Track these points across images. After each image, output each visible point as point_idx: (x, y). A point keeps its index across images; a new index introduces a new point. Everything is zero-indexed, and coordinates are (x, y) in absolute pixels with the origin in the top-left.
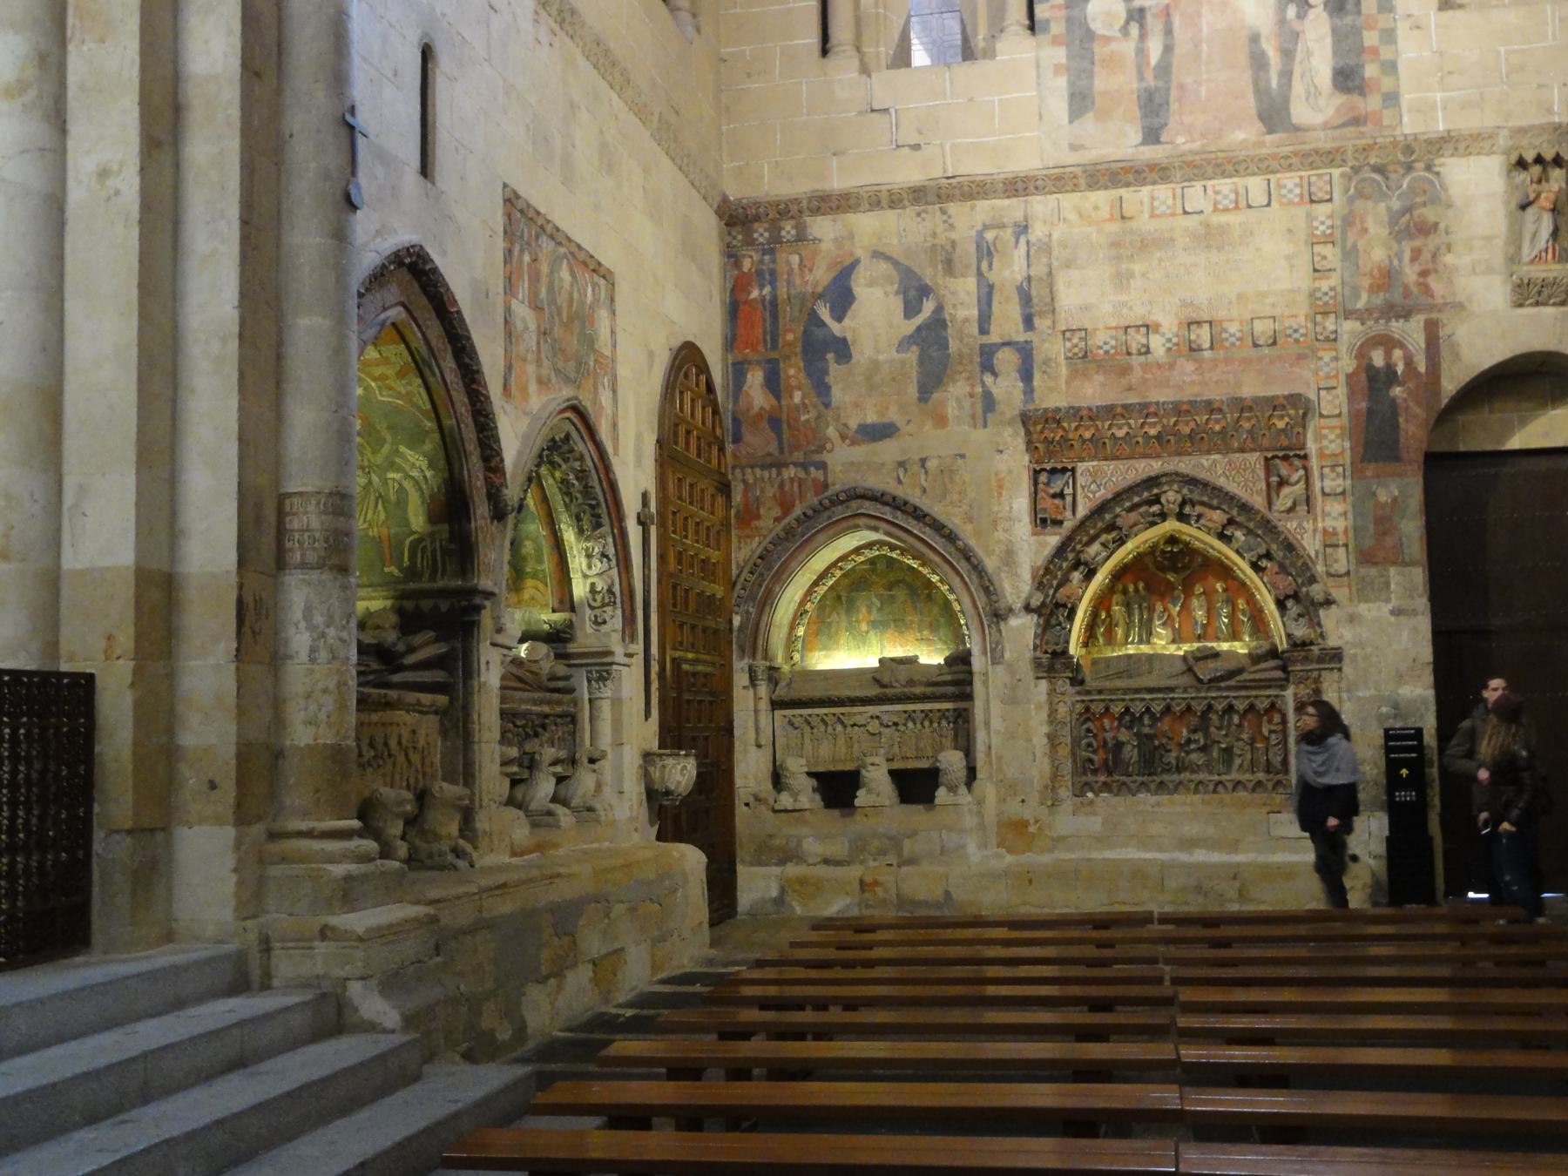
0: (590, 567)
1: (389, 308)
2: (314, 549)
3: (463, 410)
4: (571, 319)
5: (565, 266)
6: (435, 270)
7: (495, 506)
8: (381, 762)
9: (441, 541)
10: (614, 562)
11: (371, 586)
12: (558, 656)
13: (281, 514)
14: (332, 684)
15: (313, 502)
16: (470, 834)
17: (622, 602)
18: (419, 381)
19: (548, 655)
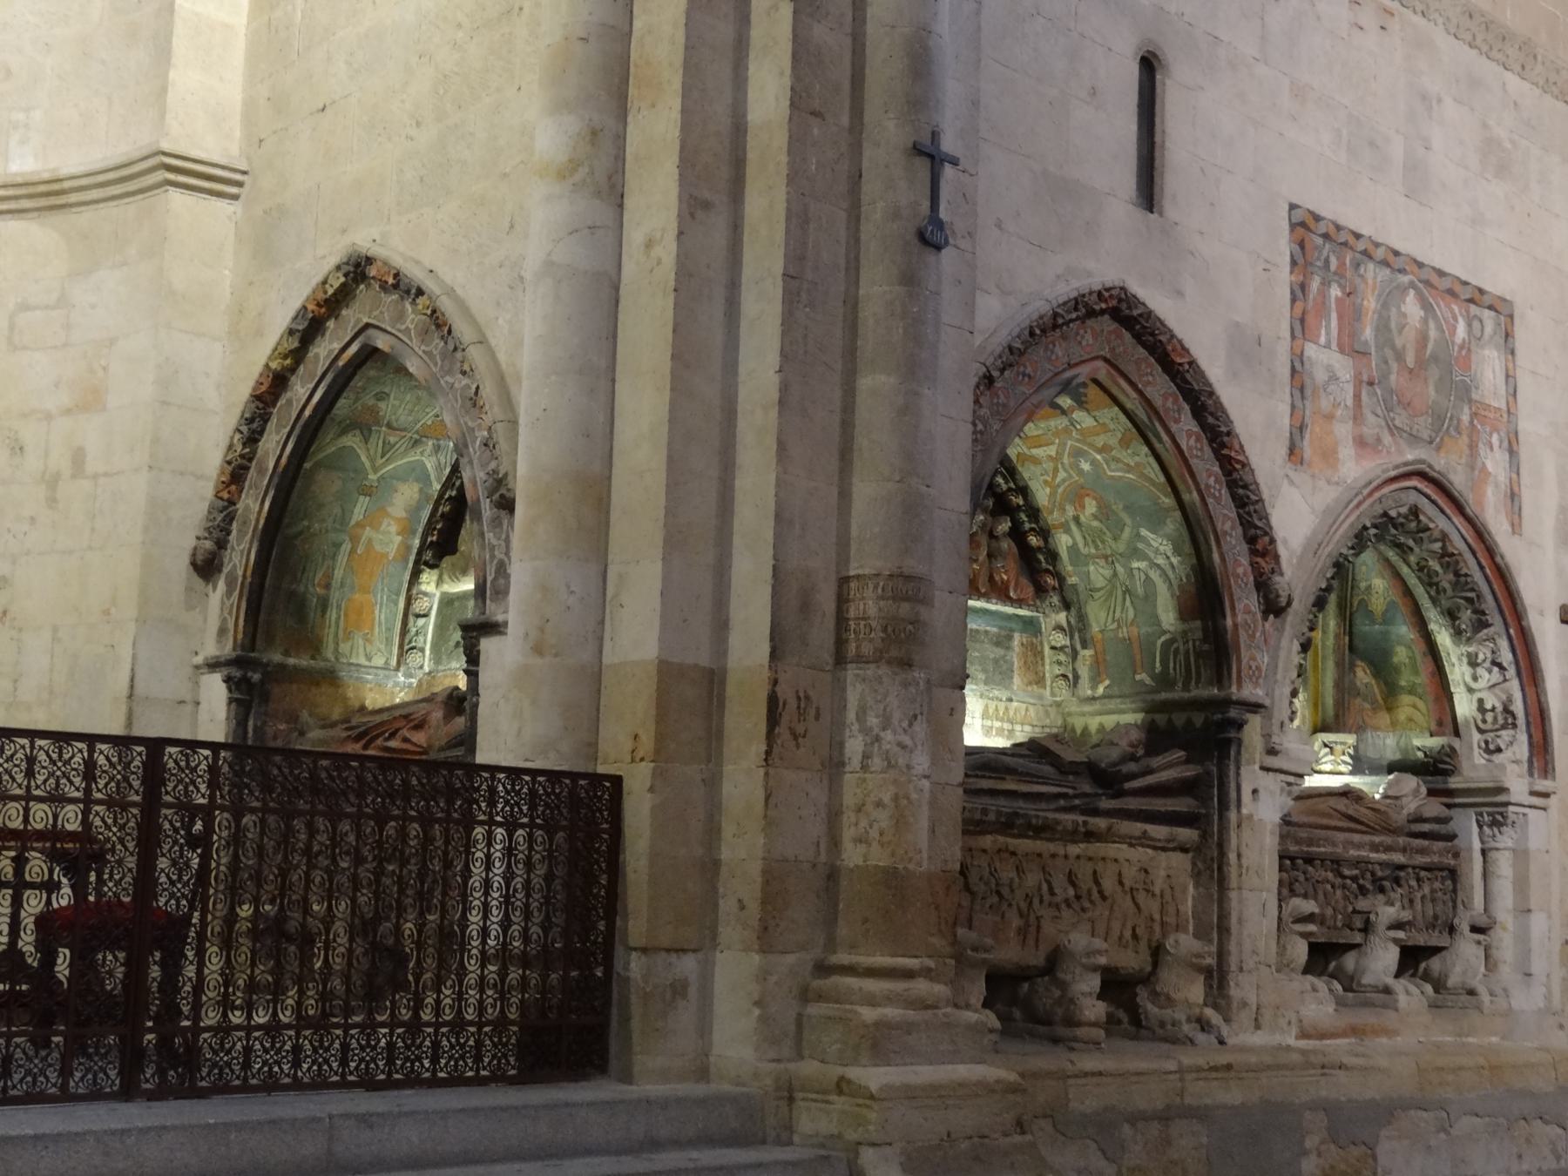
0: (1475, 679)
1: (1077, 365)
2: (871, 641)
3: (1212, 481)
4: (1422, 363)
5: (1412, 292)
6: (1149, 314)
7: (1266, 597)
8: (1087, 904)
9: (1194, 641)
10: (1511, 672)
11: (1120, 697)
12: (1432, 793)
13: (842, 600)
14: (887, 798)
15: (871, 586)
16: (1223, 1002)
17: (1528, 724)
18: (1145, 449)
19: (1416, 791)
